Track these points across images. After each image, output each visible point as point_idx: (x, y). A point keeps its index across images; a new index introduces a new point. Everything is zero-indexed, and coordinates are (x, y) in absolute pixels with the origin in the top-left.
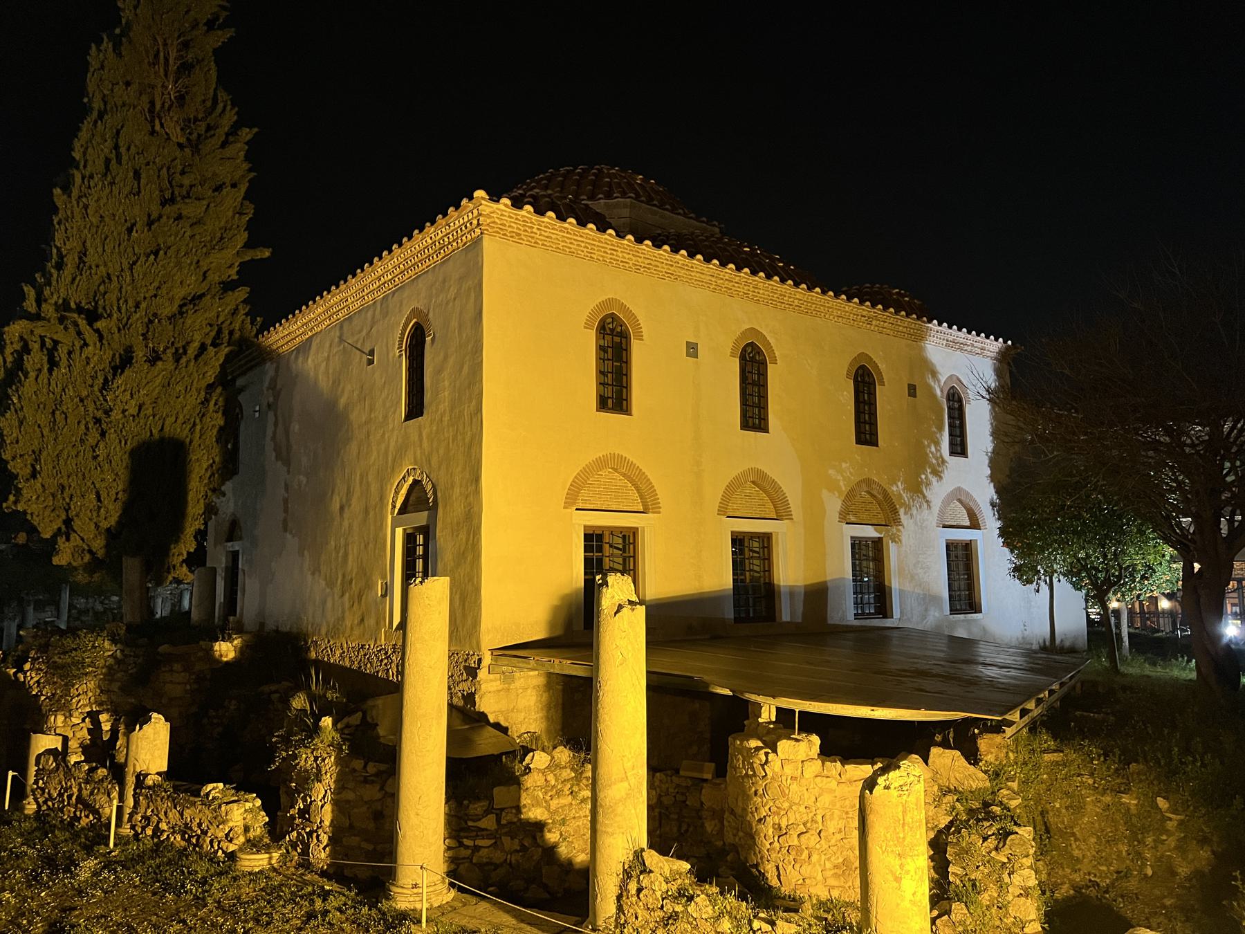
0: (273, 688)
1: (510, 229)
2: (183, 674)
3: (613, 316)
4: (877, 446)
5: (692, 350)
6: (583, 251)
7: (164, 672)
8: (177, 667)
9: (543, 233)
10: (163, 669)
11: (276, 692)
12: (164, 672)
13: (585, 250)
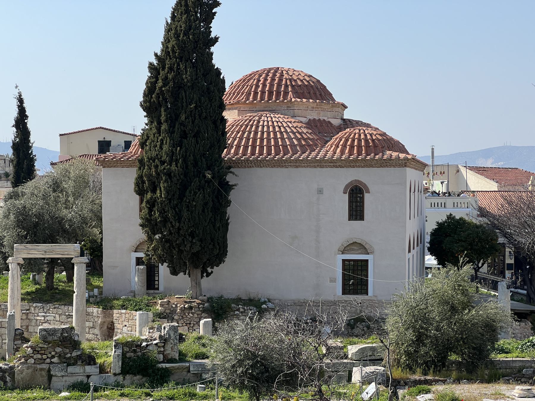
7: (265, 315)
10: (266, 314)
12: (265, 315)
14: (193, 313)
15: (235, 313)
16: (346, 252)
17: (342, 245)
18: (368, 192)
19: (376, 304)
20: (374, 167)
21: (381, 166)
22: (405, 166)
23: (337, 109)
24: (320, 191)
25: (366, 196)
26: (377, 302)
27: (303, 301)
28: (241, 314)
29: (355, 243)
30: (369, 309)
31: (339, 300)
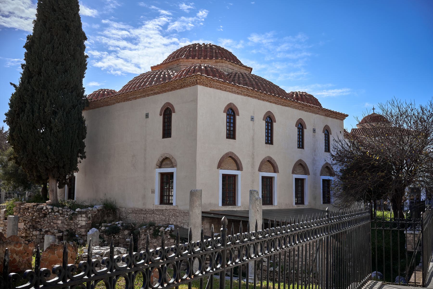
0: (117, 223)
1: (205, 83)
2: (86, 218)
3: (231, 109)
4: (304, 149)
5: (252, 119)
6: (224, 89)
8: (84, 215)
9: (214, 84)
10: (79, 216)
11: (119, 224)
13: (224, 88)
14: (29, 212)
15: (55, 214)
16: (163, 166)
17: (159, 160)
18: (174, 112)
19: (178, 214)
20: (178, 89)
21: (181, 88)
22: (197, 84)
23: (222, 64)
24: (147, 116)
25: (173, 114)
26: (178, 211)
27: (137, 210)
28: (59, 215)
29: (166, 158)
30: (173, 217)
31: (156, 209)
